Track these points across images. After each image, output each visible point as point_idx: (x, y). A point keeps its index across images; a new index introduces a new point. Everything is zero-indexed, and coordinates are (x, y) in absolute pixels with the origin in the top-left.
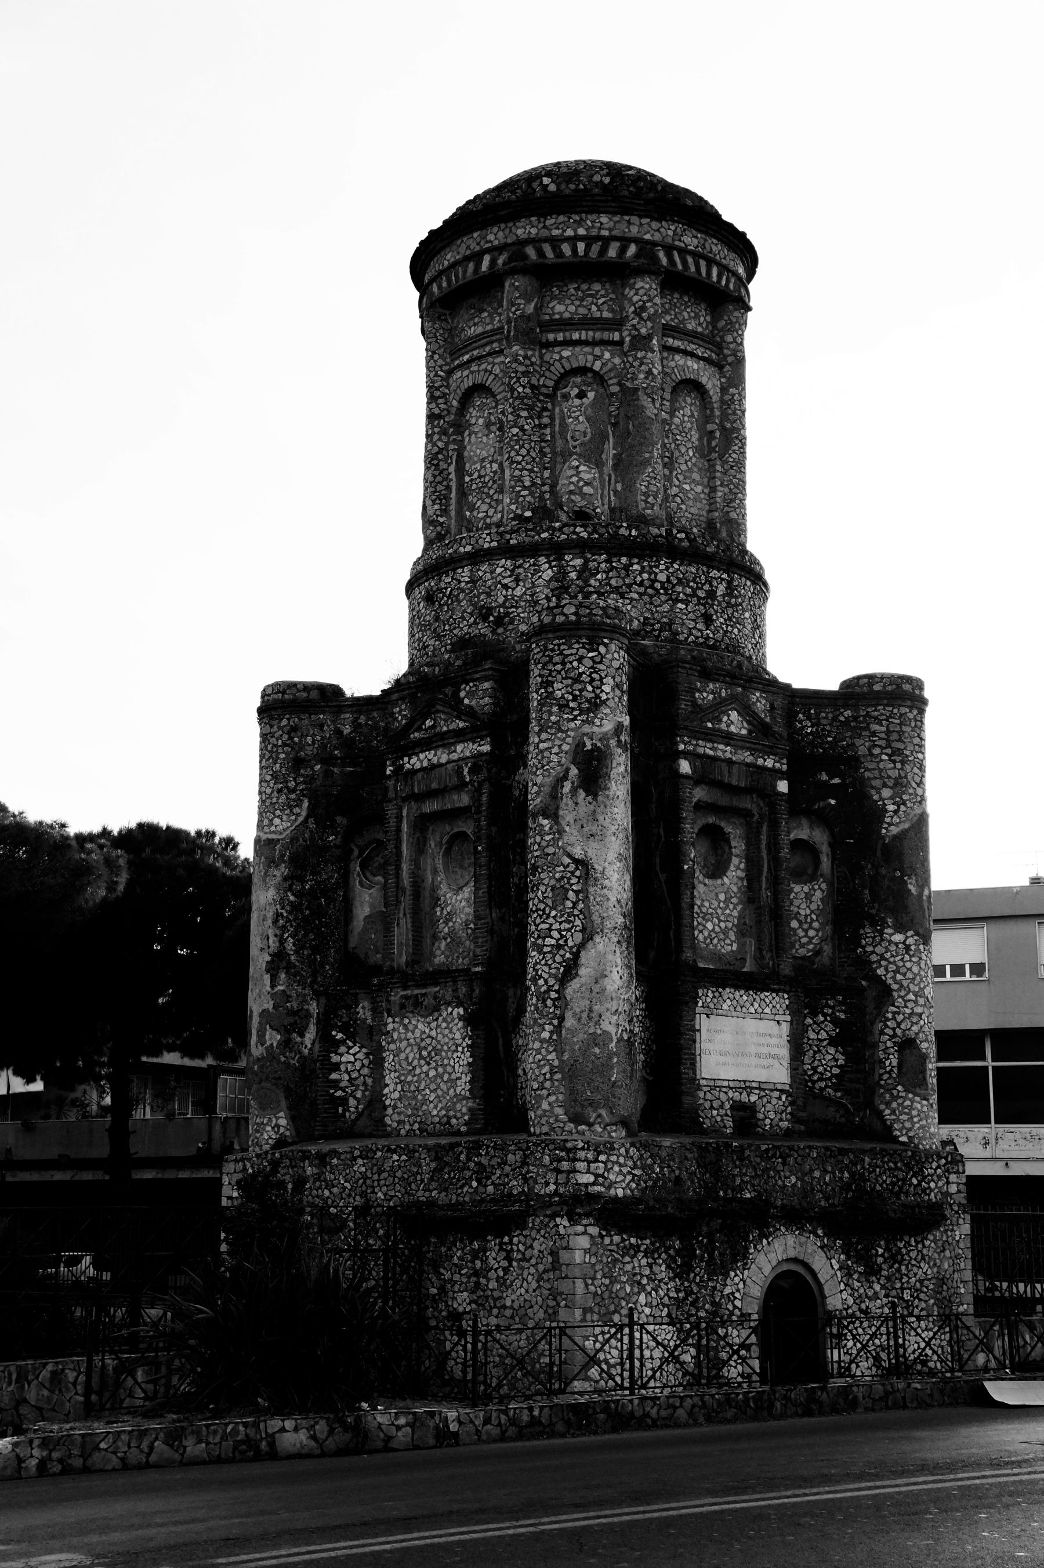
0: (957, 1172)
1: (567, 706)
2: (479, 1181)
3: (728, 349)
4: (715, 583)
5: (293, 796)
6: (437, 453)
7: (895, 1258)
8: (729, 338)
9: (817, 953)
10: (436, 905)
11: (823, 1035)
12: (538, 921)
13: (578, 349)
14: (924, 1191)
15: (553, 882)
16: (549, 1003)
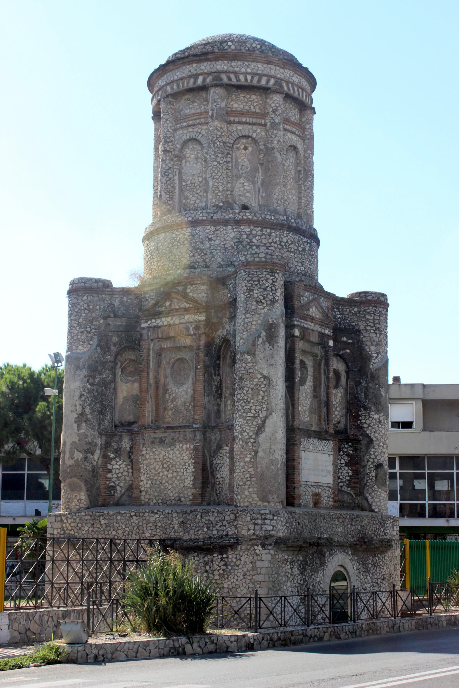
0: (397, 526)
1: (260, 302)
2: (208, 528)
3: (307, 131)
4: (305, 244)
5: (89, 335)
6: (168, 170)
7: (375, 565)
8: (308, 127)
9: (339, 422)
10: (166, 393)
11: (343, 461)
12: (243, 404)
13: (245, 126)
15: (252, 386)
16: (250, 444)
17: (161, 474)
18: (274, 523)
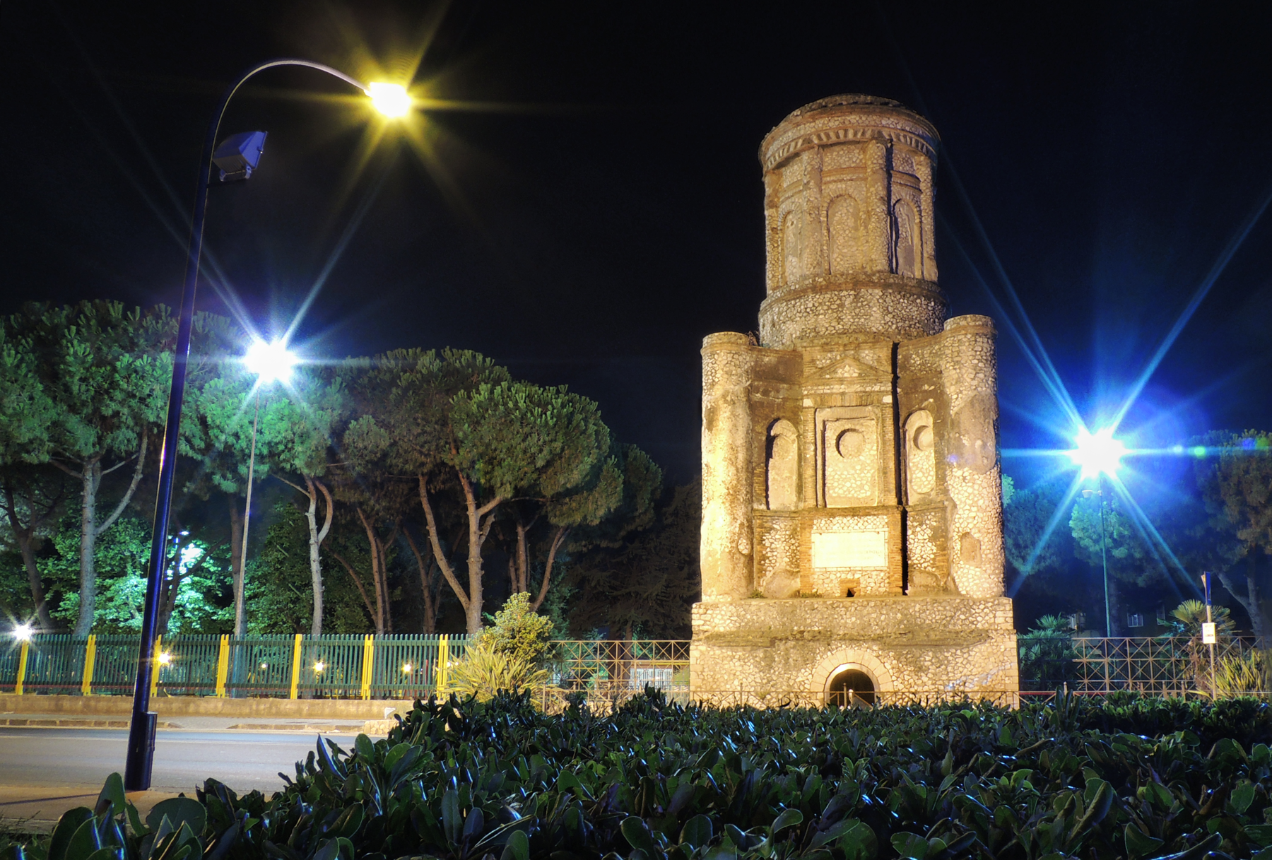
14: (972, 623)
18: (708, 617)
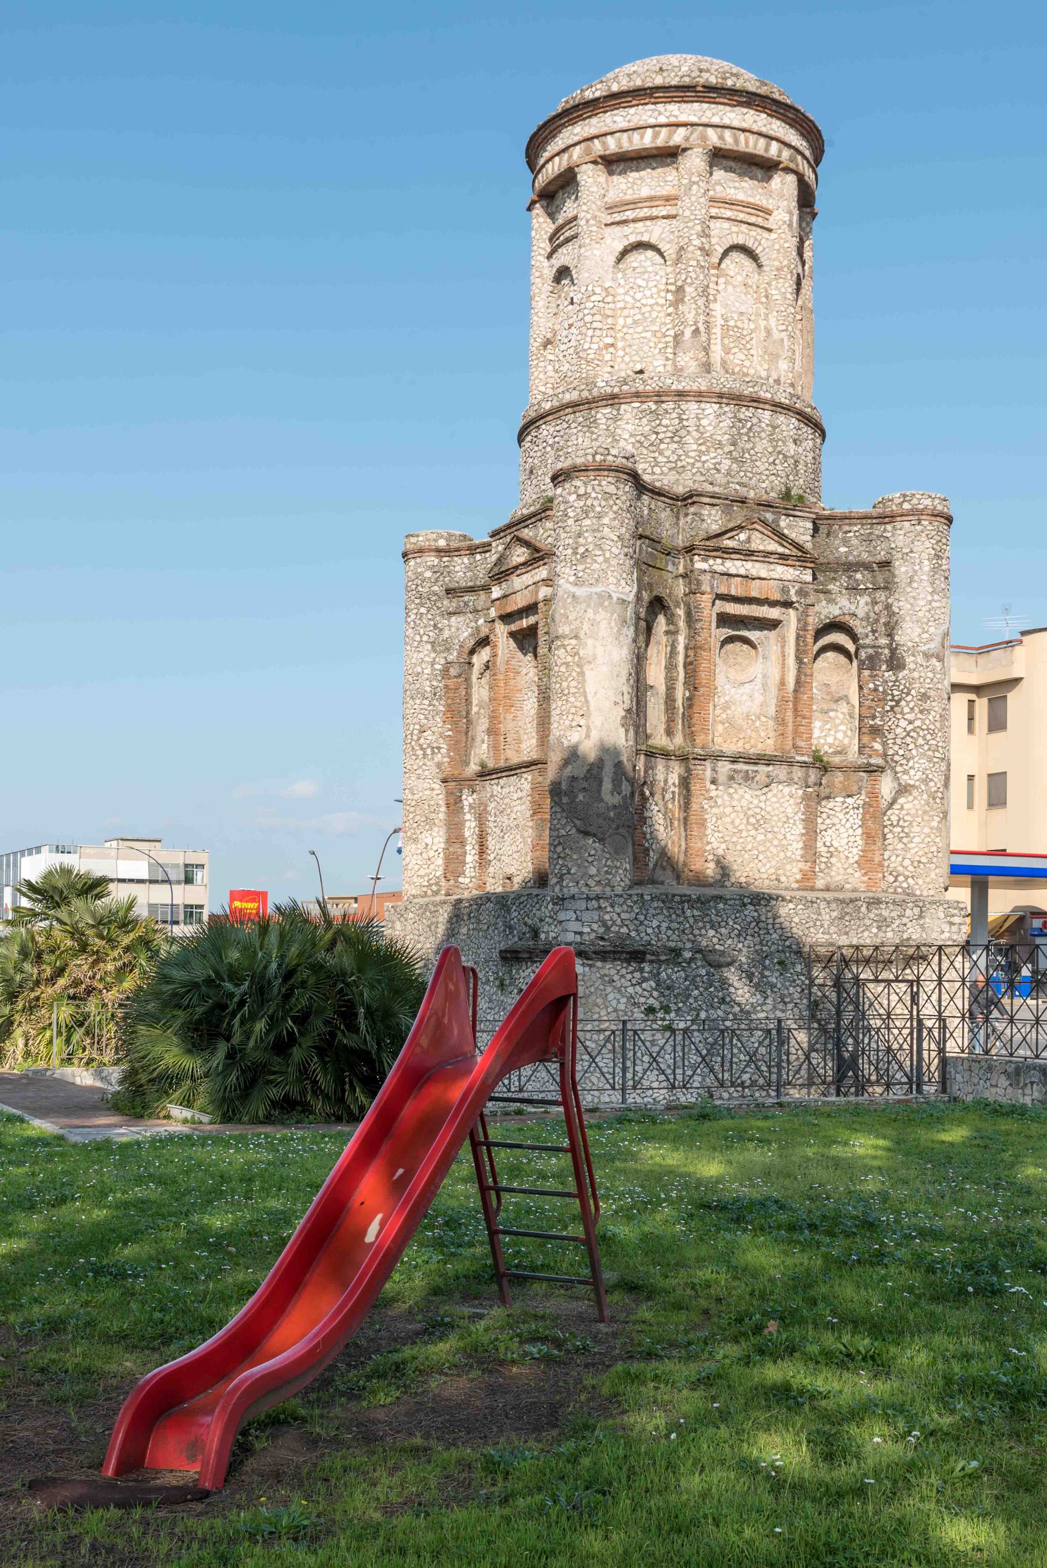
2: (879, 928)
17: (744, 834)
